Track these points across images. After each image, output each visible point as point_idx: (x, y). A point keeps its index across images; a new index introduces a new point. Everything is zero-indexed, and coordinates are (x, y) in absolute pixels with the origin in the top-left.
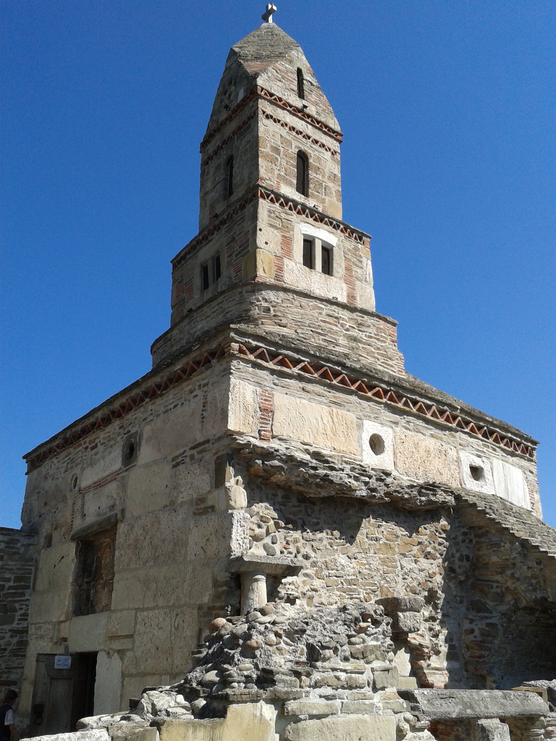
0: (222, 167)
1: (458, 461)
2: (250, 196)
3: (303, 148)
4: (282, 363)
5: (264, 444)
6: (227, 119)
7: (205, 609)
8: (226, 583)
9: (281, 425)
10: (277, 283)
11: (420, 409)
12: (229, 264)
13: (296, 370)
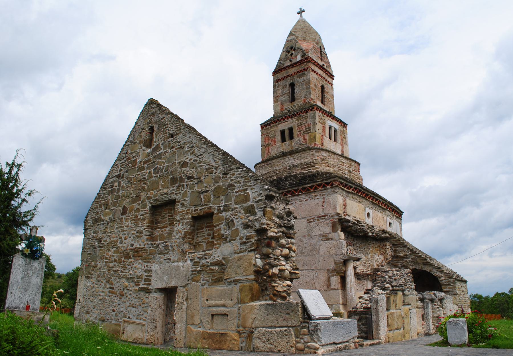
1: (386, 221)
3: (323, 84)
4: (348, 188)
6: (290, 65)
9: (349, 211)
10: (321, 147)
11: (378, 203)
12: (299, 135)
13: (351, 191)
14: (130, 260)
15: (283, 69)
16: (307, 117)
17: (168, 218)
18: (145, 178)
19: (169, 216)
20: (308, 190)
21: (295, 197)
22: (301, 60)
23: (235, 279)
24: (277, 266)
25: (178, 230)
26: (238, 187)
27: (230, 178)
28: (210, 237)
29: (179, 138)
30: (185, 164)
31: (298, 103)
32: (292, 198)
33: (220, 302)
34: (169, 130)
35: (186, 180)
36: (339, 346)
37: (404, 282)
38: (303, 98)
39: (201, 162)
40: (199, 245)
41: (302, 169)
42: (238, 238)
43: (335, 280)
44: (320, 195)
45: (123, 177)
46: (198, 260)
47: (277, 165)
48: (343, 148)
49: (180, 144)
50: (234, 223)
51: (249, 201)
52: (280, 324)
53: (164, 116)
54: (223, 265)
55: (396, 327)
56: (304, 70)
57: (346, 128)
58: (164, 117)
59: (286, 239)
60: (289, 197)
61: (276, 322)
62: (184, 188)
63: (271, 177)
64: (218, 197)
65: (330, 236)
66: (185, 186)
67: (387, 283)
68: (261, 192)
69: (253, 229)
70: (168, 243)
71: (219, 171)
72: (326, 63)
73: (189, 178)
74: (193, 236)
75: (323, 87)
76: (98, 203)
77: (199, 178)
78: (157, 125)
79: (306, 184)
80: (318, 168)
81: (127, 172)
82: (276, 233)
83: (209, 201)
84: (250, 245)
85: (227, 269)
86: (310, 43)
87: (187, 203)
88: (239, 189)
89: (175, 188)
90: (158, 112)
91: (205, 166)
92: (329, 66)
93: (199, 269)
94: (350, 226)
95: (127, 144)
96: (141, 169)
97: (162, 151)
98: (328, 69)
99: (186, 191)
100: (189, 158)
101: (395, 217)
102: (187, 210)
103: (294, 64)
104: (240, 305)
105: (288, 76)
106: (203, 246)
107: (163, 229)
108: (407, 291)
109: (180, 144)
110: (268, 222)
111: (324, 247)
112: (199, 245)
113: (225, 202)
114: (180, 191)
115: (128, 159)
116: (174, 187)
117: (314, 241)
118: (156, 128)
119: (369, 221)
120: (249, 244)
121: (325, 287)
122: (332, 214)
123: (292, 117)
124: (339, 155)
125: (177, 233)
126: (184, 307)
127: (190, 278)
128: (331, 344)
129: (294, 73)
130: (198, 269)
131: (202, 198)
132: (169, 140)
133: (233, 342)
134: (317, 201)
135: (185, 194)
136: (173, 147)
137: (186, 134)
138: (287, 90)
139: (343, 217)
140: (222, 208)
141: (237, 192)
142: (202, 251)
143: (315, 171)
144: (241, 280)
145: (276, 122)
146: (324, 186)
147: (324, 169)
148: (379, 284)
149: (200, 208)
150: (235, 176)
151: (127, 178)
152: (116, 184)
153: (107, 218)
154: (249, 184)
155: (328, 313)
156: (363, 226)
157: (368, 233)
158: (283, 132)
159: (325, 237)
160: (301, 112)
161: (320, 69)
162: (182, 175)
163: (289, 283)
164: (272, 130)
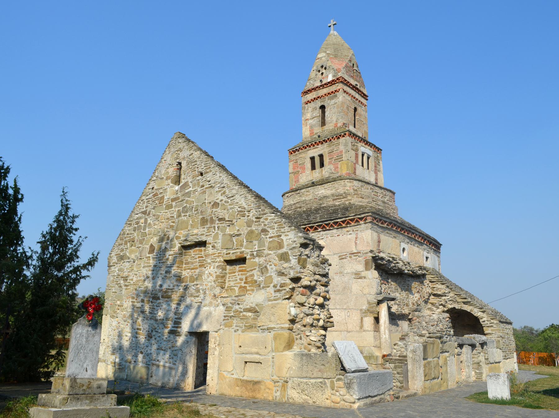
0: (318, 109)
1: (423, 255)
2: (342, 134)
3: (356, 106)
4: (382, 223)
5: (379, 255)
6: (321, 86)
7: (364, 311)
8: (375, 303)
12: (330, 163)
13: (385, 225)
14: (158, 301)
15: (313, 89)
16: (339, 144)
17: (198, 260)
18: (173, 217)
19: (199, 257)
20: (340, 225)
21: (326, 232)
22: (333, 81)
23: (269, 326)
24: (312, 315)
25: (210, 273)
26: (272, 233)
27: (263, 222)
28: (243, 282)
29: (209, 176)
30: (216, 205)
31: (329, 127)
32: (324, 233)
33: (254, 350)
34: (198, 168)
35: (217, 222)
36: (374, 399)
37: (442, 328)
38: (334, 122)
39: (233, 204)
40: (231, 289)
41: (334, 200)
42: (272, 285)
43: (369, 321)
44: (353, 231)
45: (149, 214)
46: (230, 305)
47: (307, 195)
48: (376, 175)
49: (210, 183)
50: (267, 270)
51: (283, 247)
52: (315, 375)
53: (192, 152)
54: (256, 312)
55: (433, 377)
56: (336, 91)
57: (380, 153)
58: (192, 154)
59: (321, 287)
60: (320, 231)
61: (311, 373)
62: (215, 230)
63: (300, 207)
64: (251, 242)
65: (363, 274)
66: (216, 228)
67: (424, 329)
68: (295, 239)
69: (288, 277)
70: (199, 286)
71: (251, 215)
72: (359, 82)
73: (220, 220)
74: (225, 280)
75: (355, 109)
76: (123, 240)
77: (232, 221)
78: (185, 162)
79: (337, 219)
80: (351, 200)
81: (154, 209)
82: (311, 282)
83: (242, 245)
84: (285, 293)
85: (261, 316)
86: (343, 61)
87: (219, 245)
88: (272, 235)
89: (205, 229)
90: (186, 147)
91: (237, 208)
92: (363, 85)
93: (232, 314)
94: (383, 265)
95: (153, 179)
96: (169, 207)
97: (191, 189)
98: (362, 89)
99: (217, 233)
100: (219, 197)
101: (432, 250)
102: (219, 253)
103: (325, 84)
104: (274, 354)
105: (318, 97)
106: (235, 291)
107: (193, 271)
108: (445, 338)
109: (210, 183)
110: (302, 270)
111: (356, 286)
112: (231, 289)
113: (259, 247)
114: (211, 233)
115: (154, 196)
116: (204, 228)
117: (346, 279)
118: (184, 164)
119: (404, 256)
120: (284, 291)
121: (358, 328)
122: (365, 252)
123: (322, 143)
124: (373, 185)
125: (208, 277)
126: (217, 353)
127: (223, 323)
128: (366, 397)
130: (230, 315)
131: (234, 241)
132: (198, 178)
133: (267, 390)
134: (349, 236)
135: (216, 237)
136: (203, 186)
137: (217, 173)
138: (318, 112)
139: (377, 254)
140: (255, 253)
141: (270, 238)
142: (235, 296)
143: (347, 202)
144: (275, 328)
145: (306, 148)
146: (357, 221)
147: (355, 201)
148: (415, 330)
149: (232, 252)
150: (268, 221)
151: (154, 215)
152: (142, 221)
153: (133, 256)
154: (282, 230)
155: (363, 364)
156: (398, 263)
157: (404, 270)
158: (313, 159)
159: (358, 276)
160: (333, 138)
161: (353, 89)
162: (213, 215)
163: (323, 332)
164: (301, 156)
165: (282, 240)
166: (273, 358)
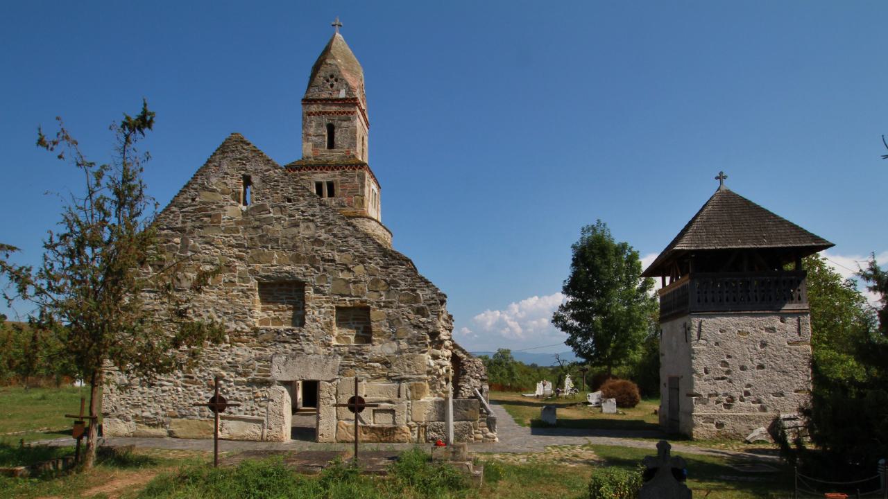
123: (333, 170)
129: (335, 112)
133: (404, 435)
141: (401, 290)
158: (319, 186)
165: (418, 295)
166: (408, 406)
